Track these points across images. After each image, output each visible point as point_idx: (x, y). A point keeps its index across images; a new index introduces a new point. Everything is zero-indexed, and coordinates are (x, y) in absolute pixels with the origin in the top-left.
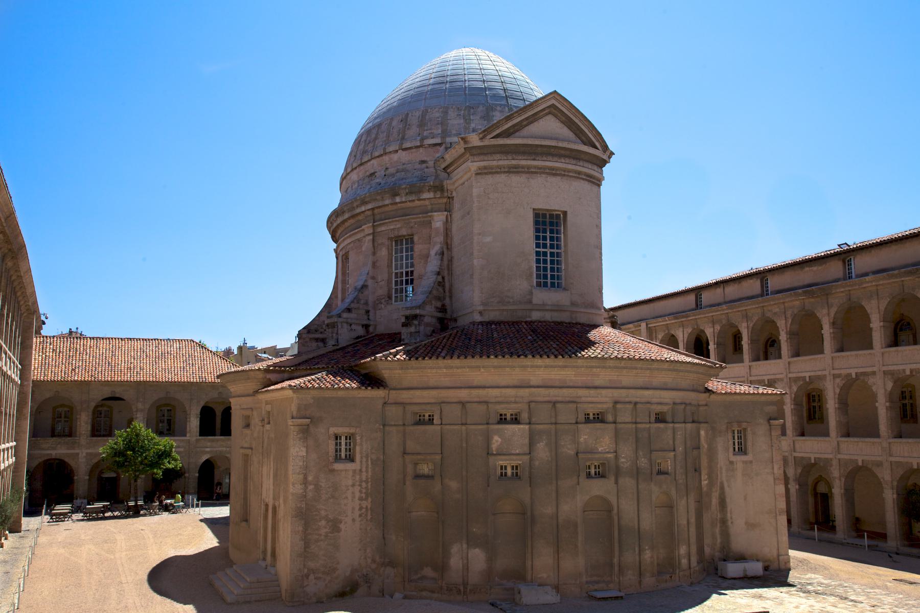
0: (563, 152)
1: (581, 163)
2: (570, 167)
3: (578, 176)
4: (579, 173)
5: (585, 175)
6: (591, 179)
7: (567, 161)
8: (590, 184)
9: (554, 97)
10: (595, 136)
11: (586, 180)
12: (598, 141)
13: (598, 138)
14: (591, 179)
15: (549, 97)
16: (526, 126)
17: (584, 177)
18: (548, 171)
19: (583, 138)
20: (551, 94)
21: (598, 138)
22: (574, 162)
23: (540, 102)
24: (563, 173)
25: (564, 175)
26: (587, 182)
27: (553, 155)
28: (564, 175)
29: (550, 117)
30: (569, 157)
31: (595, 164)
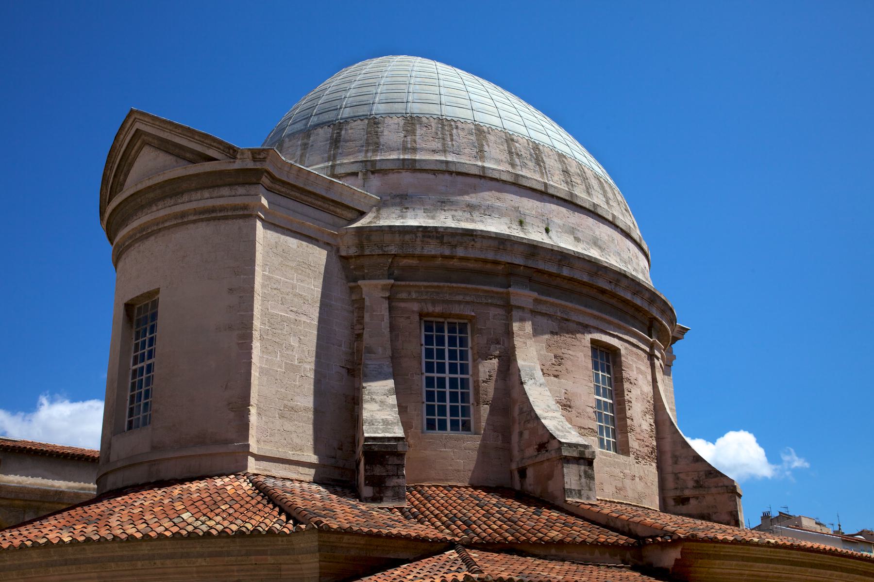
0: (151, 195)
1: (186, 197)
2: (162, 213)
3: (180, 221)
4: (183, 215)
5: (195, 214)
6: (214, 215)
7: (161, 205)
8: (212, 223)
9: (135, 118)
10: (202, 143)
11: (202, 220)
12: (210, 146)
13: (208, 142)
14: (214, 215)
15: (129, 123)
16: (125, 180)
17: (194, 218)
18: (138, 235)
19: (188, 155)
20: (129, 116)
21: (208, 142)
22: (172, 202)
23: (122, 137)
24: (155, 228)
25: (160, 230)
26: (205, 223)
27: (142, 207)
28: (160, 230)
29: (146, 150)
30: (162, 198)
31: (219, 186)
